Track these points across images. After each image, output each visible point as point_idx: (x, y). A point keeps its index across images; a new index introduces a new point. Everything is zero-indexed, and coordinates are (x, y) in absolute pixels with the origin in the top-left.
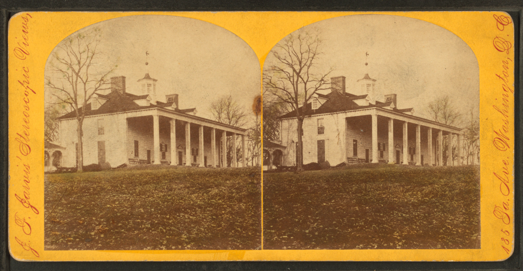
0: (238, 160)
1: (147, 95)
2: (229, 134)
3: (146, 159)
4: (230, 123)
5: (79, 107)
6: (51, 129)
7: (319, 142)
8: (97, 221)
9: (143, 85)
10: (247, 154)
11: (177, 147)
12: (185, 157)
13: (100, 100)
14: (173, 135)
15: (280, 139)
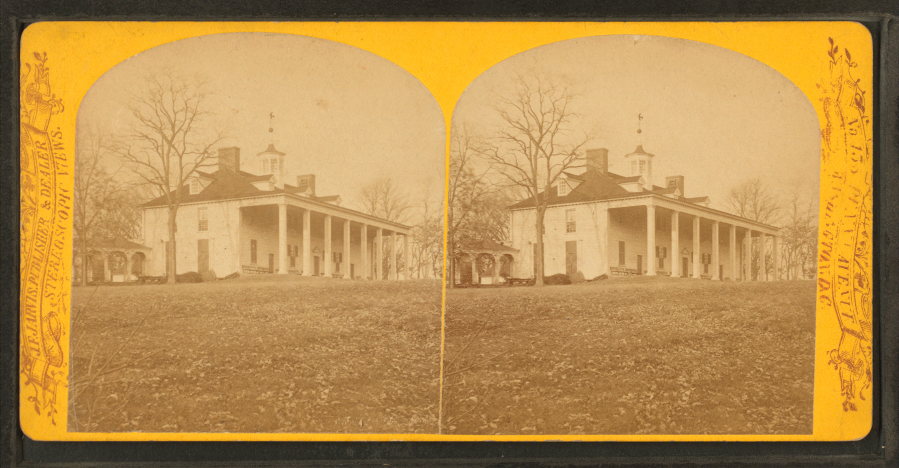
0: (398, 271)
1: (271, 176)
2: (387, 233)
3: (636, 268)
4: (388, 217)
5: (172, 190)
6: (499, 223)
7: (568, 244)
8: (558, 356)
9: (265, 161)
10: (411, 262)
11: (313, 251)
12: (324, 266)
13: (202, 181)
14: (307, 233)
15: (511, 239)
